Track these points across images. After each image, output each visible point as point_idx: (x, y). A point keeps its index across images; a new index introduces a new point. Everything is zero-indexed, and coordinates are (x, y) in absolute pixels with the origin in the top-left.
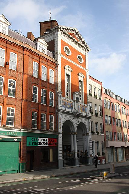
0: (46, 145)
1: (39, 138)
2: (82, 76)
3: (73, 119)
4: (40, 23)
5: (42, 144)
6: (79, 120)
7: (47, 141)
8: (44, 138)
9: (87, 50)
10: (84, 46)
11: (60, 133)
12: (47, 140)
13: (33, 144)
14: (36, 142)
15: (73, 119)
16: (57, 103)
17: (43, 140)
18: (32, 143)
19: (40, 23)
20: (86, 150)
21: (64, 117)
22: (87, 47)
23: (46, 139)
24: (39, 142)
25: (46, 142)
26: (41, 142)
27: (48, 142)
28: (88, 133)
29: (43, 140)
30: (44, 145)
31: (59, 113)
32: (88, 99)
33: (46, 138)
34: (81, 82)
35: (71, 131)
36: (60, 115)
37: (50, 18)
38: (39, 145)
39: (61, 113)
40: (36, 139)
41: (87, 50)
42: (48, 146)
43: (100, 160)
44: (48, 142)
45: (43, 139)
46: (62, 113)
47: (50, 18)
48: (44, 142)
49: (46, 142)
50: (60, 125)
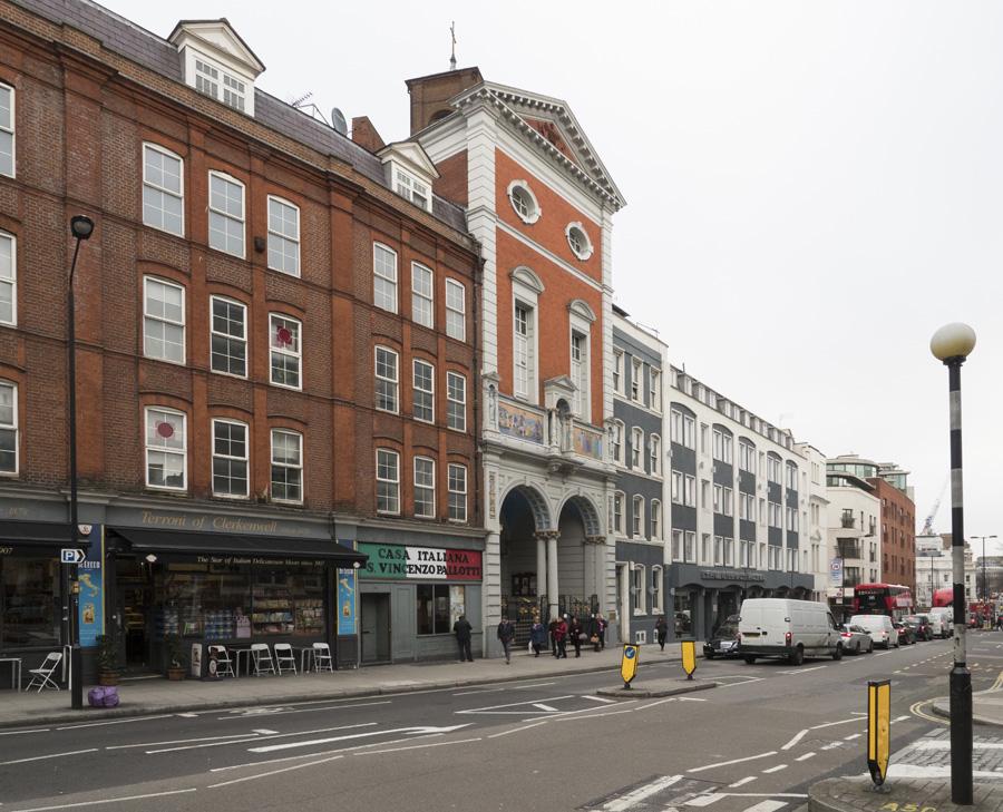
0: (435, 576)
1: (407, 549)
2: (583, 312)
4: (406, 82)
6: (567, 486)
7: (439, 560)
8: (429, 551)
9: (607, 204)
10: (599, 187)
11: (489, 533)
12: (442, 556)
13: (383, 570)
14: (397, 562)
15: (547, 483)
16: (478, 421)
17: (423, 557)
18: (381, 564)
19: (406, 82)
20: (595, 596)
21: (507, 474)
23: (435, 551)
24: (408, 562)
25: (435, 564)
26: (419, 563)
27: (444, 564)
28: (602, 534)
29: (423, 557)
30: (429, 576)
31: (489, 457)
34: (579, 337)
35: (537, 526)
37: (453, 60)
38: (409, 575)
40: (397, 552)
41: (611, 200)
42: (444, 576)
44: (444, 564)
45: (425, 553)
46: (501, 456)
47: (453, 60)
48: (429, 563)
49: (435, 564)
50: (492, 502)
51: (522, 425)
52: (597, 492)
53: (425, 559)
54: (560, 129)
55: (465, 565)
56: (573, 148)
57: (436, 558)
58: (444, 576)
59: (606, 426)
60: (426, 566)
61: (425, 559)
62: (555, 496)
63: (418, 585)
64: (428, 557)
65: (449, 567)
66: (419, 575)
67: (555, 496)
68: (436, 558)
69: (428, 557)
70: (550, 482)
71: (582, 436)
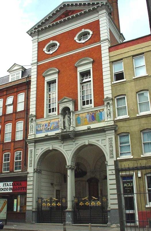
0: (8, 191)
3: (61, 144)
5: (3, 190)
6: (76, 142)
7: (10, 186)
12: (11, 184)
15: (63, 145)
17: (4, 185)
22: (98, 3)
23: (9, 183)
25: (8, 187)
26: (3, 188)
27: (12, 187)
29: (4, 185)
30: (6, 191)
32: (105, 93)
33: (10, 182)
36: (31, 147)
39: (33, 144)
42: (11, 191)
44: (12, 187)
45: (5, 184)
48: (6, 187)
49: (8, 187)
52: (100, 139)
53: (5, 186)
54: (70, 9)
56: (74, 8)
57: (9, 185)
59: (105, 104)
60: (5, 188)
61: (5, 186)
62: (68, 151)
64: (6, 185)
65: (14, 188)
67: (68, 151)
68: (9, 185)
69: (6, 185)
70: (64, 144)
71: (88, 116)
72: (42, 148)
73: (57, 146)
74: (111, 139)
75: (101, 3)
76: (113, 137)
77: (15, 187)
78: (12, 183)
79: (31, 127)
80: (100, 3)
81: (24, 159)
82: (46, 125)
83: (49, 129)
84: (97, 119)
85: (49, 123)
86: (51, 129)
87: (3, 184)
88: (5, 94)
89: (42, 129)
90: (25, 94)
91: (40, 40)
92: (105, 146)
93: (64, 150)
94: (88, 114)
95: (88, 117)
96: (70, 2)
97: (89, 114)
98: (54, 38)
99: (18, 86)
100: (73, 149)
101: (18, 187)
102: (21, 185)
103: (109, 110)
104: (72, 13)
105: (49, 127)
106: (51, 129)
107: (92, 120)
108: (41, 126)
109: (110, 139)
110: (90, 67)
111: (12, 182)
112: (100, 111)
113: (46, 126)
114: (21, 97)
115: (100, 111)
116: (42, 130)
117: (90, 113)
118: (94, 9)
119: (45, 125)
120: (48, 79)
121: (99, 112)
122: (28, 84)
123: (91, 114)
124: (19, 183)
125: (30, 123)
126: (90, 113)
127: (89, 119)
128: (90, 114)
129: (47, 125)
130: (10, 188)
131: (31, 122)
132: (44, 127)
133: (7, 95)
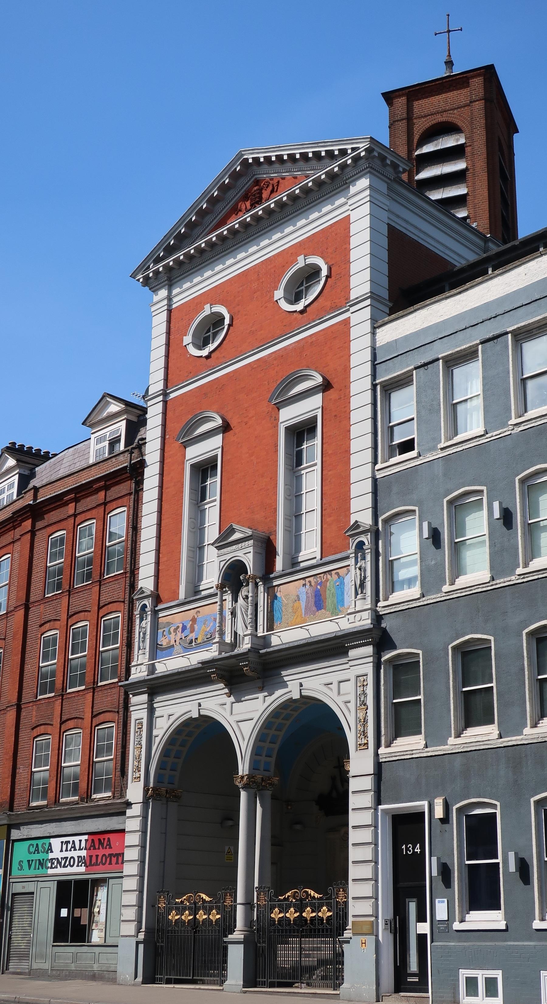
11: (129, 804)
12: (83, 844)
13: (30, 866)
14: (41, 856)
17: (64, 847)
18: (29, 861)
22: (343, 153)
24: (51, 856)
25: (75, 854)
29: (64, 847)
30: (69, 870)
37: (449, 64)
38: (50, 871)
42: (82, 869)
43: (498, 974)
44: (84, 853)
47: (449, 64)
48: (69, 854)
49: (75, 854)
51: (192, 630)
53: (66, 850)
55: (107, 852)
57: (77, 847)
58: (82, 869)
60: (66, 858)
61: (66, 850)
63: (60, 883)
64: (70, 846)
65: (91, 857)
66: (60, 870)
68: (77, 847)
72: (170, 712)
73: (214, 702)
74: (365, 677)
75: (353, 149)
76: (369, 669)
77: (94, 853)
78: (86, 841)
79: (141, 633)
80: (349, 151)
81: (119, 753)
82: (184, 628)
83: (191, 642)
84: (329, 602)
85: (194, 620)
86: (199, 641)
87: (62, 842)
88: (71, 512)
89: (172, 642)
90: (128, 511)
91: (177, 302)
92: (348, 704)
93: (232, 719)
94: (304, 585)
95: (303, 598)
96: (221, 176)
97: (308, 586)
98: (212, 296)
99: (108, 483)
100: (256, 716)
101: (101, 852)
102: (111, 848)
103: (360, 569)
104: (272, 192)
105: (192, 636)
106: (199, 641)
107: (314, 608)
108: (170, 633)
109: (362, 679)
110: (312, 405)
111: (86, 837)
112: (338, 574)
113: (187, 632)
114: (118, 522)
115: (338, 574)
116: (173, 646)
117: (310, 582)
118: (332, 176)
119: (181, 626)
120: (196, 453)
121: (335, 577)
122: (136, 471)
123: (313, 584)
124: (104, 839)
125: (138, 621)
126: (310, 582)
127: (307, 602)
128: (310, 585)
129: (188, 626)
130: (78, 857)
131: (141, 620)
132: (179, 635)
133: (79, 514)
